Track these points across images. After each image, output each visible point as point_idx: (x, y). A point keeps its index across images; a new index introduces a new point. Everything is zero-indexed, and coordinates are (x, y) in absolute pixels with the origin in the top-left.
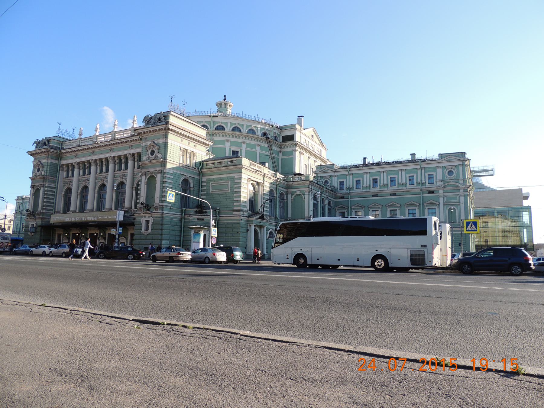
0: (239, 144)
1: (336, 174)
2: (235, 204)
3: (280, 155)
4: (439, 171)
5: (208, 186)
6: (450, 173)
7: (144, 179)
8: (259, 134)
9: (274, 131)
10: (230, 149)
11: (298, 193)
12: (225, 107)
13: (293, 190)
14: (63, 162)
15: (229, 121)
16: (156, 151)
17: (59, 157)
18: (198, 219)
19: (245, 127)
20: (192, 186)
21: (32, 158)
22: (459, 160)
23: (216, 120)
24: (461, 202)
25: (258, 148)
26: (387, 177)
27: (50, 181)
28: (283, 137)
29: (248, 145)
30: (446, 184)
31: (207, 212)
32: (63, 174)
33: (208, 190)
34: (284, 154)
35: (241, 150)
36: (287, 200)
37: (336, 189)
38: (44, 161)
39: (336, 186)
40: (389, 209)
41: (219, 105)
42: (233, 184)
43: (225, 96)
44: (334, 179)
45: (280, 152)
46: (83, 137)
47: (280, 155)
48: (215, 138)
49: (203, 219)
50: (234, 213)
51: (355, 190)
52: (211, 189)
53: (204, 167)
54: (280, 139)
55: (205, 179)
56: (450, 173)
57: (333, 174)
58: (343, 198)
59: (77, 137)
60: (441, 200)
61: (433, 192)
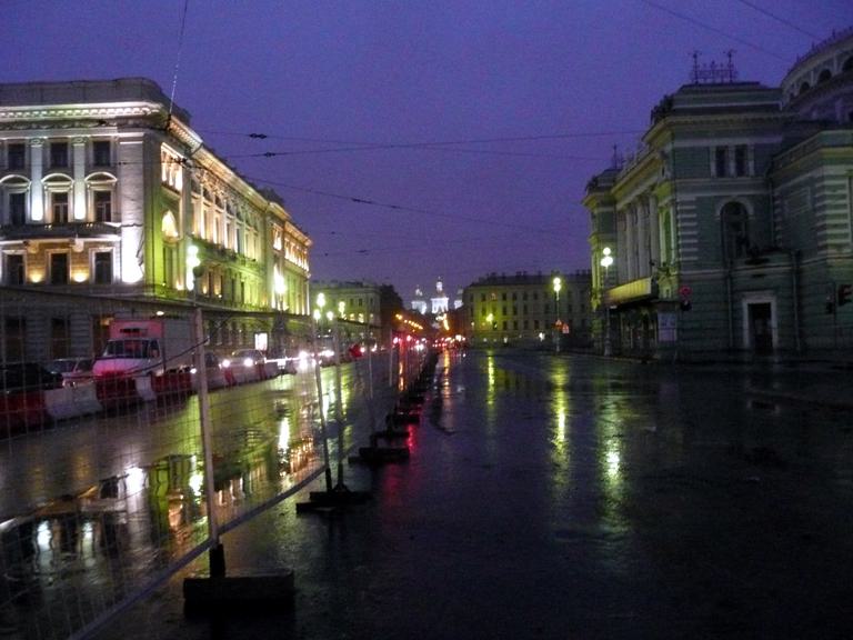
14: (620, 206)
20: (751, 211)
31: (767, 261)
42: (814, 192)
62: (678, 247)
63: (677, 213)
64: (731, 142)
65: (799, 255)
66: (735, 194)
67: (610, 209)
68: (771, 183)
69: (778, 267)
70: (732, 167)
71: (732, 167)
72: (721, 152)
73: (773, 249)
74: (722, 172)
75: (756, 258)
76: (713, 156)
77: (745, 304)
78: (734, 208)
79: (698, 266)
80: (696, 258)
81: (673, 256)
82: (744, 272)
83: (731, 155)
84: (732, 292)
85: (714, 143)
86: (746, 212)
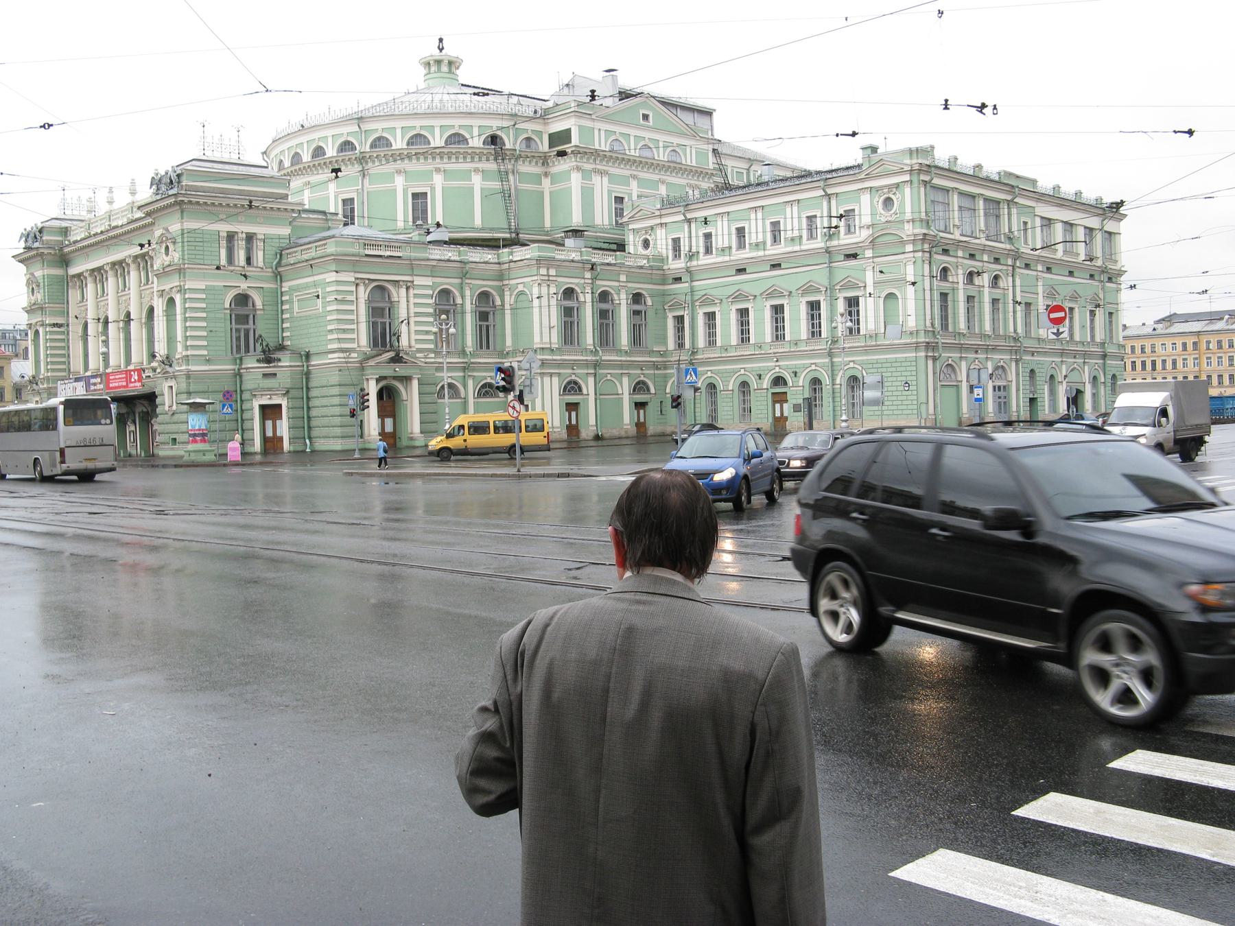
1: (664, 220)
2: (330, 337)
3: (546, 182)
4: (865, 198)
5: (290, 302)
6: (888, 202)
7: (159, 306)
8: (476, 142)
10: (405, 191)
11: (521, 288)
12: (439, 70)
13: (512, 282)
14: (73, 270)
16: (171, 247)
17: (64, 260)
18: (265, 375)
20: (259, 305)
21: (22, 268)
22: (902, 172)
25: (477, 180)
27: (54, 314)
28: (551, 136)
32: (74, 295)
33: (291, 310)
35: (433, 189)
36: (503, 305)
37: (662, 260)
38: (39, 274)
39: (664, 252)
43: (441, 40)
44: (660, 233)
45: (546, 174)
46: (116, 206)
50: (330, 356)
51: (704, 260)
52: (296, 309)
53: (284, 262)
55: (286, 286)
56: (888, 202)
57: (658, 221)
58: (678, 280)
59: (103, 208)
60: (869, 277)
61: (855, 256)
62: (186, 338)
63: (185, 300)
64: (243, 228)
65: (308, 356)
66: (244, 286)
67: (59, 272)
68: (278, 277)
70: (241, 256)
71: (241, 256)
72: (231, 237)
73: (281, 348)
77: (256, 404)
79: (208, 361)
80: (205, 353)
81: (180, 348)
85: (224, 228)
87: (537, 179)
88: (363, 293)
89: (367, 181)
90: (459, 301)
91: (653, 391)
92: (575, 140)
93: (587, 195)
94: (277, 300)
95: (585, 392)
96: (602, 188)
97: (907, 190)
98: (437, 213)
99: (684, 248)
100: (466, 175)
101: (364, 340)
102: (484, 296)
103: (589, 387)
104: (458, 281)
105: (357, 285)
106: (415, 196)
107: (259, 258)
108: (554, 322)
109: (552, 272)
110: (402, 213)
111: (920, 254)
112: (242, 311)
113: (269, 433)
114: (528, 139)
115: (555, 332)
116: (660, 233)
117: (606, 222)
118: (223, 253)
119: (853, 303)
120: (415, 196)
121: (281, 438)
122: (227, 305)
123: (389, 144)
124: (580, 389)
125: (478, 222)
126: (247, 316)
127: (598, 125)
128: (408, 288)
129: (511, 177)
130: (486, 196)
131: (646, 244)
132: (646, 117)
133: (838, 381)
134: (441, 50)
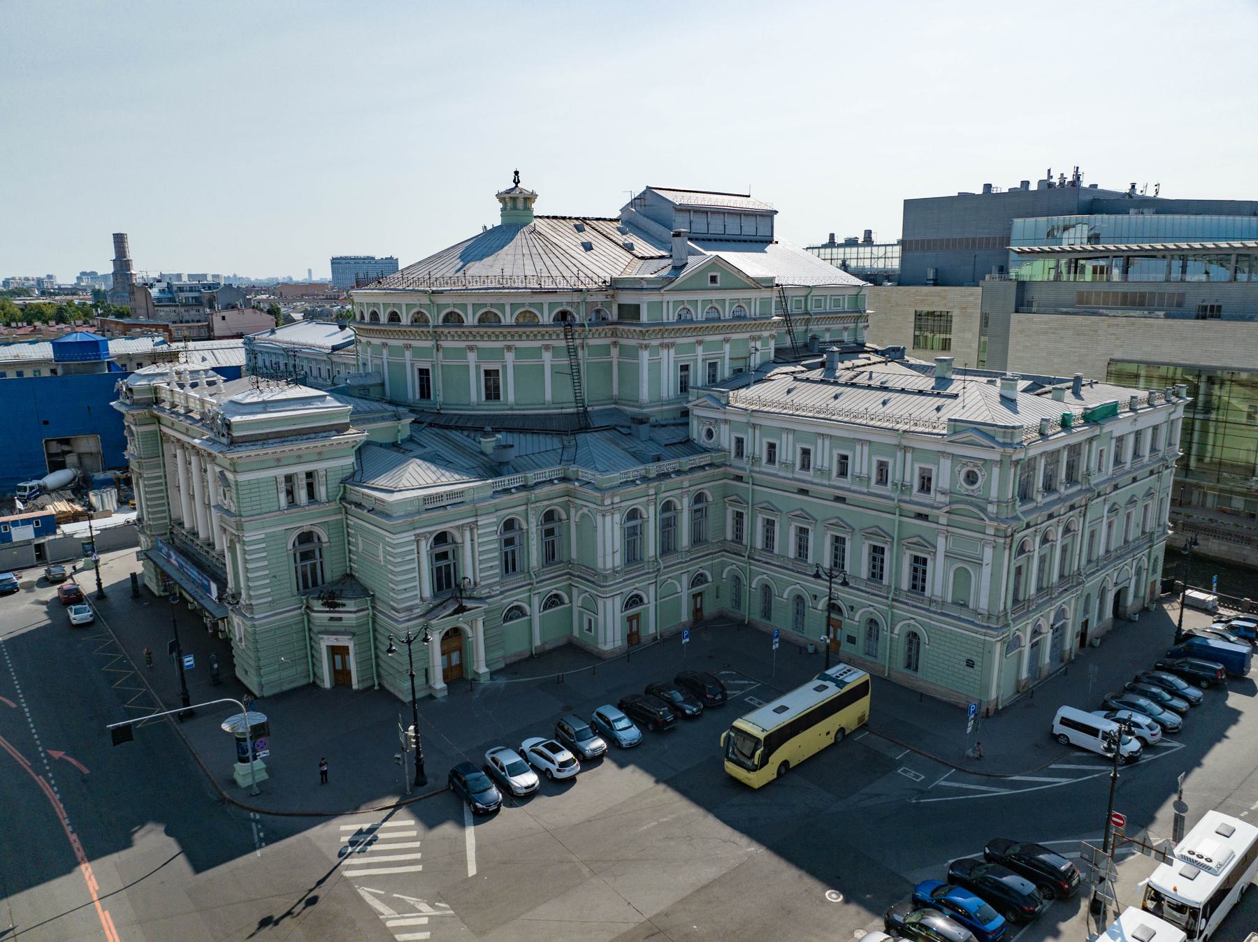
0: (497, 354)
6: (971, 478)
8: (546, 317)
9: (590, 299)
10: (478, 367)
11: (585, 510)
12: (515, 208)
15: (470, 301)
18: (331, 619)
19: (508, 309)
20: (324, 539)
23: (441, 300)
24: (985, 562)
25: (547, 356)
26: (831, 452)
29: (519, 353)
30: (955, 506)
31: (344, 605)
34: (624, 351)
35: (505, 367)
36: (568, 519)
39: (726, 446)
40: (829, 533)
41: (501, 197)
43: (516, 173)
44: (724, 429)
47: (614, 352)
48: (445, 344)
49: (340, 619)
54: (613, 314)
56: (971, 478)
57: (722, 417)
58: (739, 478)
60: (941, 543)
64: (300, 470)
66: (306, 526)
69: (351, 613)
71: (302, 495)
72: (289, 479)
74: (292, 503)
75: (332, 602)
76: (283, 486)
78: (306, 537)
82: (321, 616)
83: (302, 482)
84: (308, 633)
86: (319, 539)
87: (606, 350)
88: (425, 546)
89: (441, 354)
90: (525, 526)
91: (710, 579)
92: (644, 317)
93: (655, 367)
94: (343, 531)
95: (646, 601)
96: (669, 361)
97: (996, 471)
98: (509, 393)
99: (747, 449)
100: (537, 352)
101: (427, 593)
102: (549, 516)
103: (650, 597)
104: (523, 508)
105: (418, 541)
106: (487, 373)
107: (321, 492)
108: (618, 545)
109: (617, 500)
110: (475, 392)
111: (1002, 541)
112: (307, 547)
113: (339, 667)
114: (598, 311)
115: (618, 557)
116: (724, 429)
117: (671, 393)
118: (283, 496)
119: (920, 562)
120: (487, 373)
121: (349, 673)
122: (290, 546)
123: (460, 320)
124: (641, 600)
125: (548, 397)
126: (313, 552)
127: (667, 297)
128: (471, 530)
129: (580, 352)
130: (556, 372)
131: (710, 434)
132: (713, 279)
133: (896, 631)
134: (517, 182)
